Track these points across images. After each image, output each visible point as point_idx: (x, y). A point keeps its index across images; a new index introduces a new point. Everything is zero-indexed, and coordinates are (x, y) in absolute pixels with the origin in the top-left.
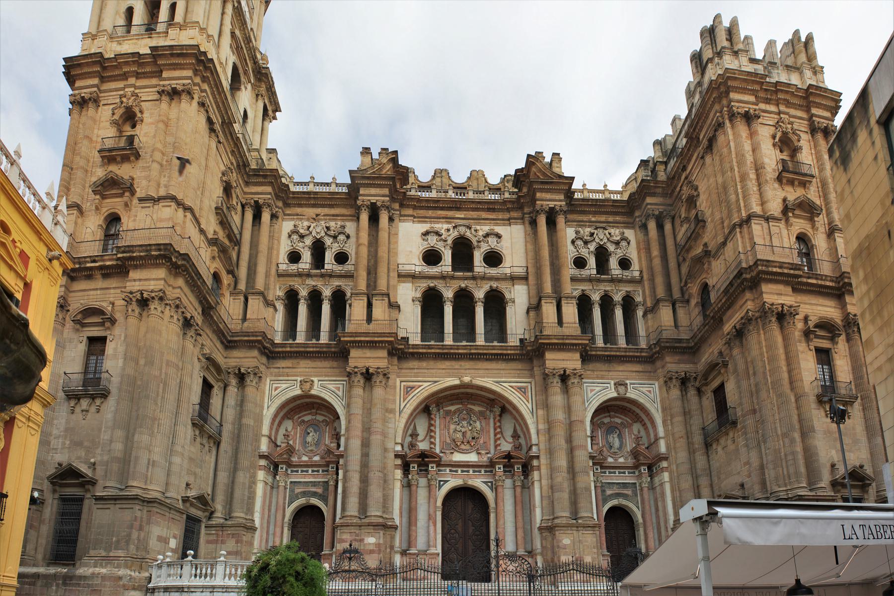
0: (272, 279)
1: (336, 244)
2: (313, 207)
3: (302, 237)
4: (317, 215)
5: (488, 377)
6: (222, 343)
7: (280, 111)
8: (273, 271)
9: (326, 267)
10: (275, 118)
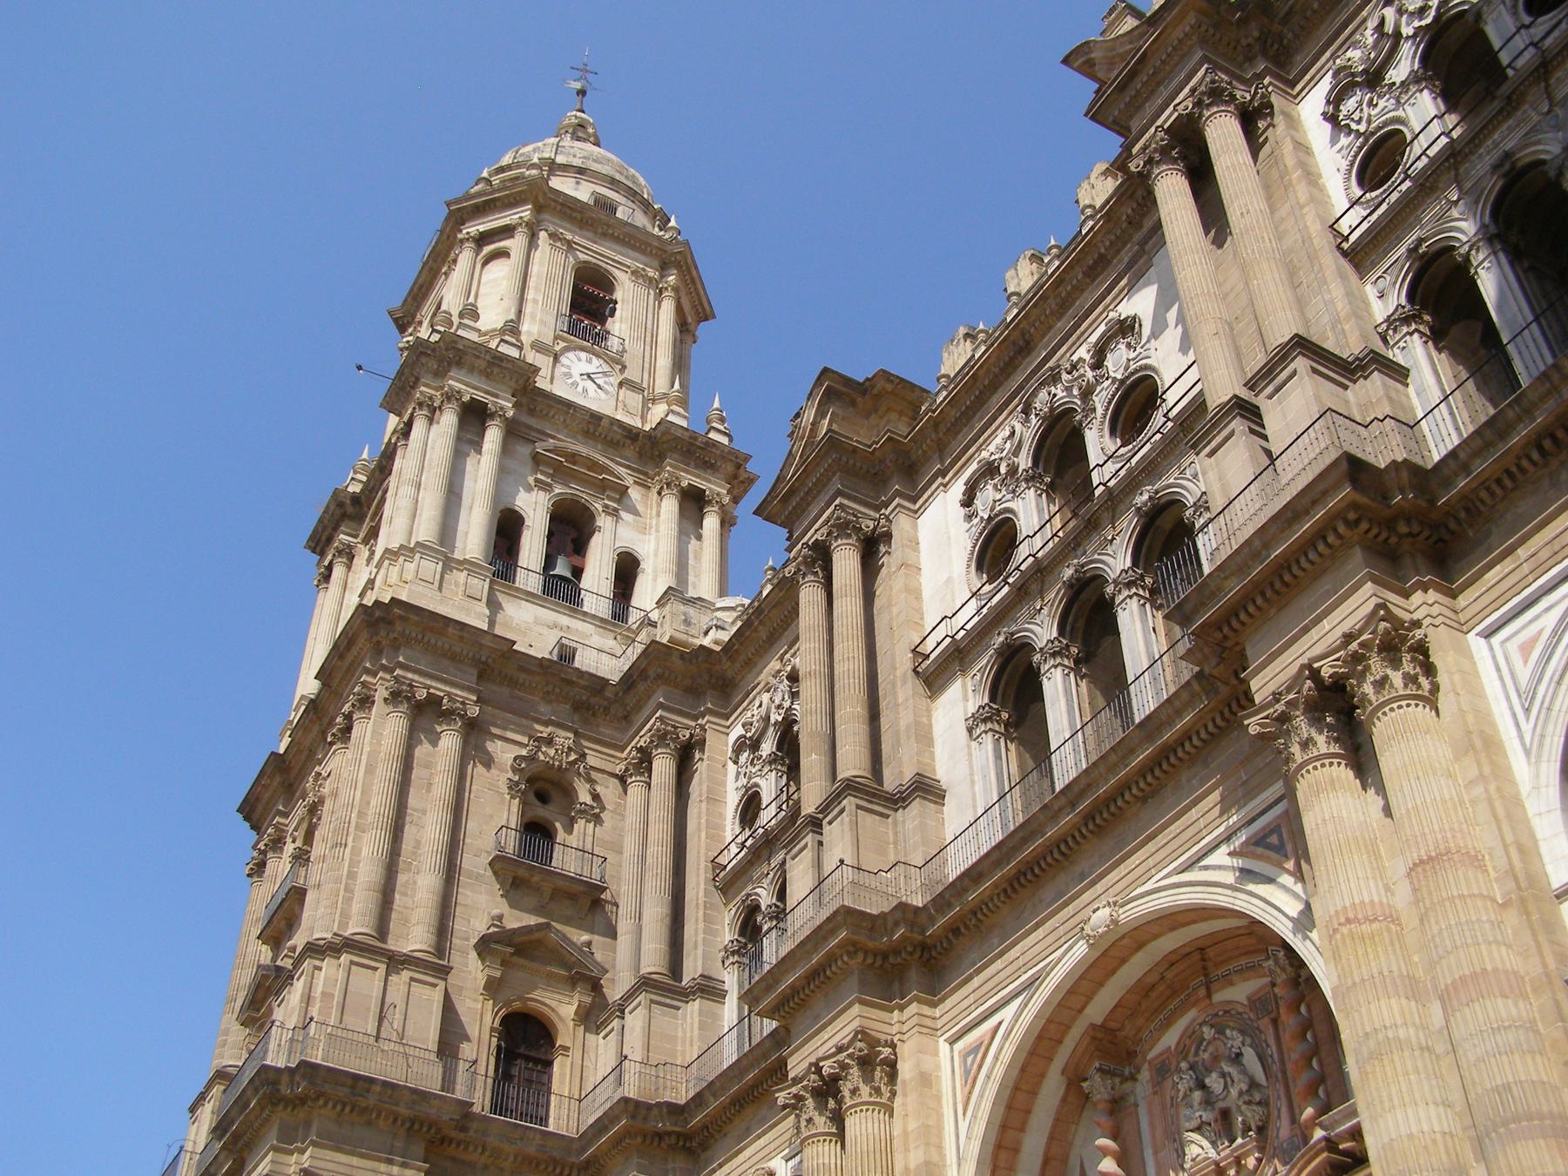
5: (1159, 866)
7: (747, 458)
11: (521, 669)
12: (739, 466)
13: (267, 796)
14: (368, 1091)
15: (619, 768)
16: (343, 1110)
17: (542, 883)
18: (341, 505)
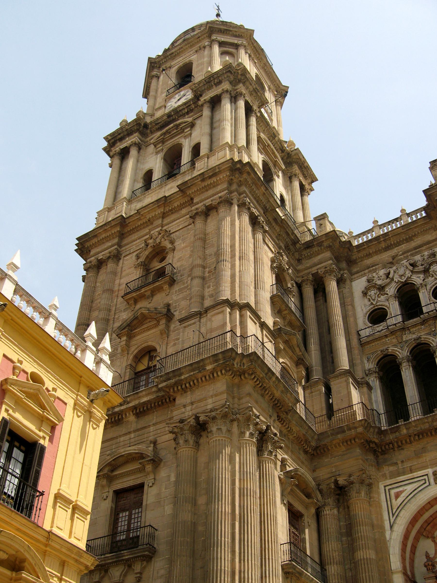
0: (356, 352)
1: (430, 279)
2: (386, 251)
3: (381, 289)
4: (393, 258)
6: (306, 452)
7: (317, 180)
8: (355, 342)
9: (425, 310)
10: (312, 190)
11: (275, 220)
12: (313, 182)
13: (103, 236)
14: (270, 378)
15: (299, 280)
16: (258, 384)
17: (288, 316)
18: (139, 124)
